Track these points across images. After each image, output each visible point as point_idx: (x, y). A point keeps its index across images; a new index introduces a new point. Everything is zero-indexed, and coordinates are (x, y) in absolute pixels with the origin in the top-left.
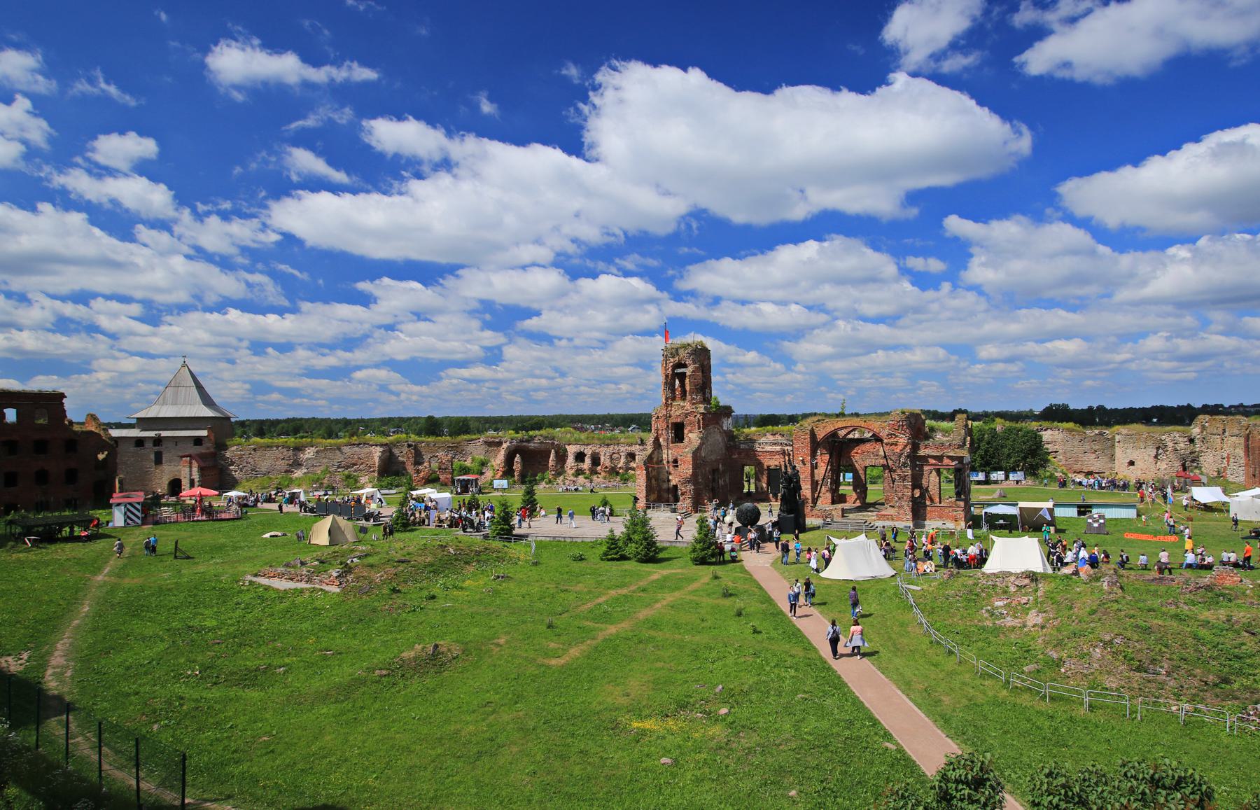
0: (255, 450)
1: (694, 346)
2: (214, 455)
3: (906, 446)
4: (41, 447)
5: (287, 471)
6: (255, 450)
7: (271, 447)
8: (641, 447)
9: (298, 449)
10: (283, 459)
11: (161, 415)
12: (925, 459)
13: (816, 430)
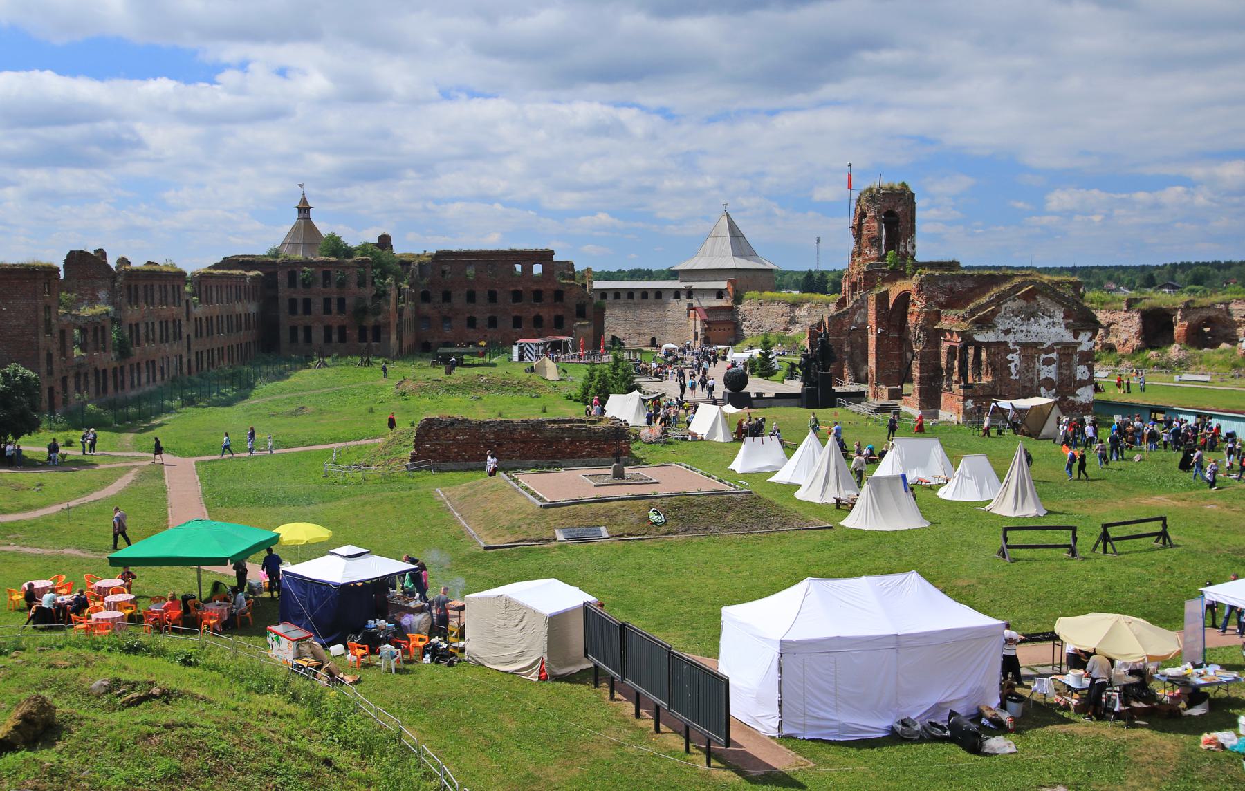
0: (761, 304)
1: (875, 191)
2: (730, 309)
3: (918, 316)
4: (538, 296)
5: (786, 329)
6: (761, 304)
7: (774, 301)
8: (1128, 315)
9: (796, 304)
10: (783, 315)
11: (694, 268)
12: (941, 332)
13: (890, 293)
